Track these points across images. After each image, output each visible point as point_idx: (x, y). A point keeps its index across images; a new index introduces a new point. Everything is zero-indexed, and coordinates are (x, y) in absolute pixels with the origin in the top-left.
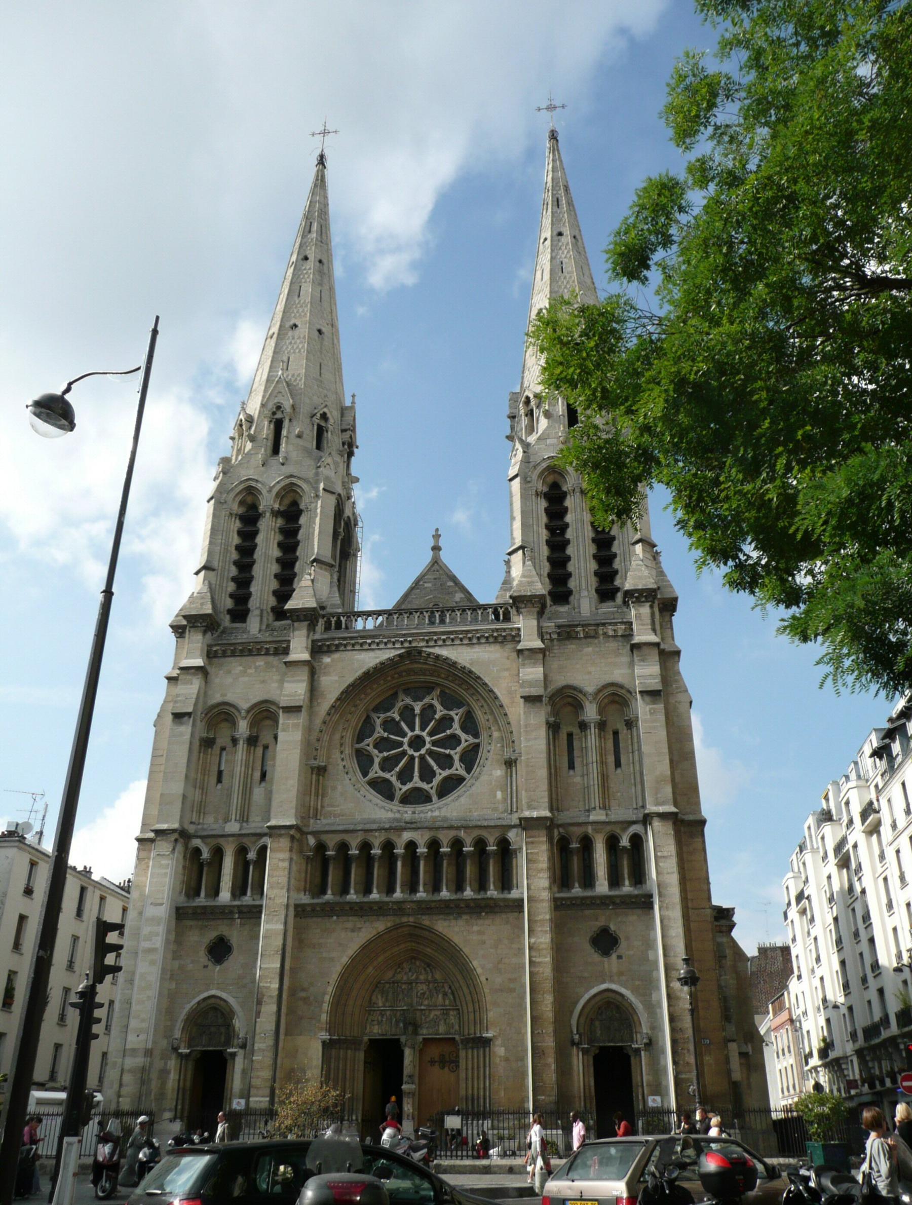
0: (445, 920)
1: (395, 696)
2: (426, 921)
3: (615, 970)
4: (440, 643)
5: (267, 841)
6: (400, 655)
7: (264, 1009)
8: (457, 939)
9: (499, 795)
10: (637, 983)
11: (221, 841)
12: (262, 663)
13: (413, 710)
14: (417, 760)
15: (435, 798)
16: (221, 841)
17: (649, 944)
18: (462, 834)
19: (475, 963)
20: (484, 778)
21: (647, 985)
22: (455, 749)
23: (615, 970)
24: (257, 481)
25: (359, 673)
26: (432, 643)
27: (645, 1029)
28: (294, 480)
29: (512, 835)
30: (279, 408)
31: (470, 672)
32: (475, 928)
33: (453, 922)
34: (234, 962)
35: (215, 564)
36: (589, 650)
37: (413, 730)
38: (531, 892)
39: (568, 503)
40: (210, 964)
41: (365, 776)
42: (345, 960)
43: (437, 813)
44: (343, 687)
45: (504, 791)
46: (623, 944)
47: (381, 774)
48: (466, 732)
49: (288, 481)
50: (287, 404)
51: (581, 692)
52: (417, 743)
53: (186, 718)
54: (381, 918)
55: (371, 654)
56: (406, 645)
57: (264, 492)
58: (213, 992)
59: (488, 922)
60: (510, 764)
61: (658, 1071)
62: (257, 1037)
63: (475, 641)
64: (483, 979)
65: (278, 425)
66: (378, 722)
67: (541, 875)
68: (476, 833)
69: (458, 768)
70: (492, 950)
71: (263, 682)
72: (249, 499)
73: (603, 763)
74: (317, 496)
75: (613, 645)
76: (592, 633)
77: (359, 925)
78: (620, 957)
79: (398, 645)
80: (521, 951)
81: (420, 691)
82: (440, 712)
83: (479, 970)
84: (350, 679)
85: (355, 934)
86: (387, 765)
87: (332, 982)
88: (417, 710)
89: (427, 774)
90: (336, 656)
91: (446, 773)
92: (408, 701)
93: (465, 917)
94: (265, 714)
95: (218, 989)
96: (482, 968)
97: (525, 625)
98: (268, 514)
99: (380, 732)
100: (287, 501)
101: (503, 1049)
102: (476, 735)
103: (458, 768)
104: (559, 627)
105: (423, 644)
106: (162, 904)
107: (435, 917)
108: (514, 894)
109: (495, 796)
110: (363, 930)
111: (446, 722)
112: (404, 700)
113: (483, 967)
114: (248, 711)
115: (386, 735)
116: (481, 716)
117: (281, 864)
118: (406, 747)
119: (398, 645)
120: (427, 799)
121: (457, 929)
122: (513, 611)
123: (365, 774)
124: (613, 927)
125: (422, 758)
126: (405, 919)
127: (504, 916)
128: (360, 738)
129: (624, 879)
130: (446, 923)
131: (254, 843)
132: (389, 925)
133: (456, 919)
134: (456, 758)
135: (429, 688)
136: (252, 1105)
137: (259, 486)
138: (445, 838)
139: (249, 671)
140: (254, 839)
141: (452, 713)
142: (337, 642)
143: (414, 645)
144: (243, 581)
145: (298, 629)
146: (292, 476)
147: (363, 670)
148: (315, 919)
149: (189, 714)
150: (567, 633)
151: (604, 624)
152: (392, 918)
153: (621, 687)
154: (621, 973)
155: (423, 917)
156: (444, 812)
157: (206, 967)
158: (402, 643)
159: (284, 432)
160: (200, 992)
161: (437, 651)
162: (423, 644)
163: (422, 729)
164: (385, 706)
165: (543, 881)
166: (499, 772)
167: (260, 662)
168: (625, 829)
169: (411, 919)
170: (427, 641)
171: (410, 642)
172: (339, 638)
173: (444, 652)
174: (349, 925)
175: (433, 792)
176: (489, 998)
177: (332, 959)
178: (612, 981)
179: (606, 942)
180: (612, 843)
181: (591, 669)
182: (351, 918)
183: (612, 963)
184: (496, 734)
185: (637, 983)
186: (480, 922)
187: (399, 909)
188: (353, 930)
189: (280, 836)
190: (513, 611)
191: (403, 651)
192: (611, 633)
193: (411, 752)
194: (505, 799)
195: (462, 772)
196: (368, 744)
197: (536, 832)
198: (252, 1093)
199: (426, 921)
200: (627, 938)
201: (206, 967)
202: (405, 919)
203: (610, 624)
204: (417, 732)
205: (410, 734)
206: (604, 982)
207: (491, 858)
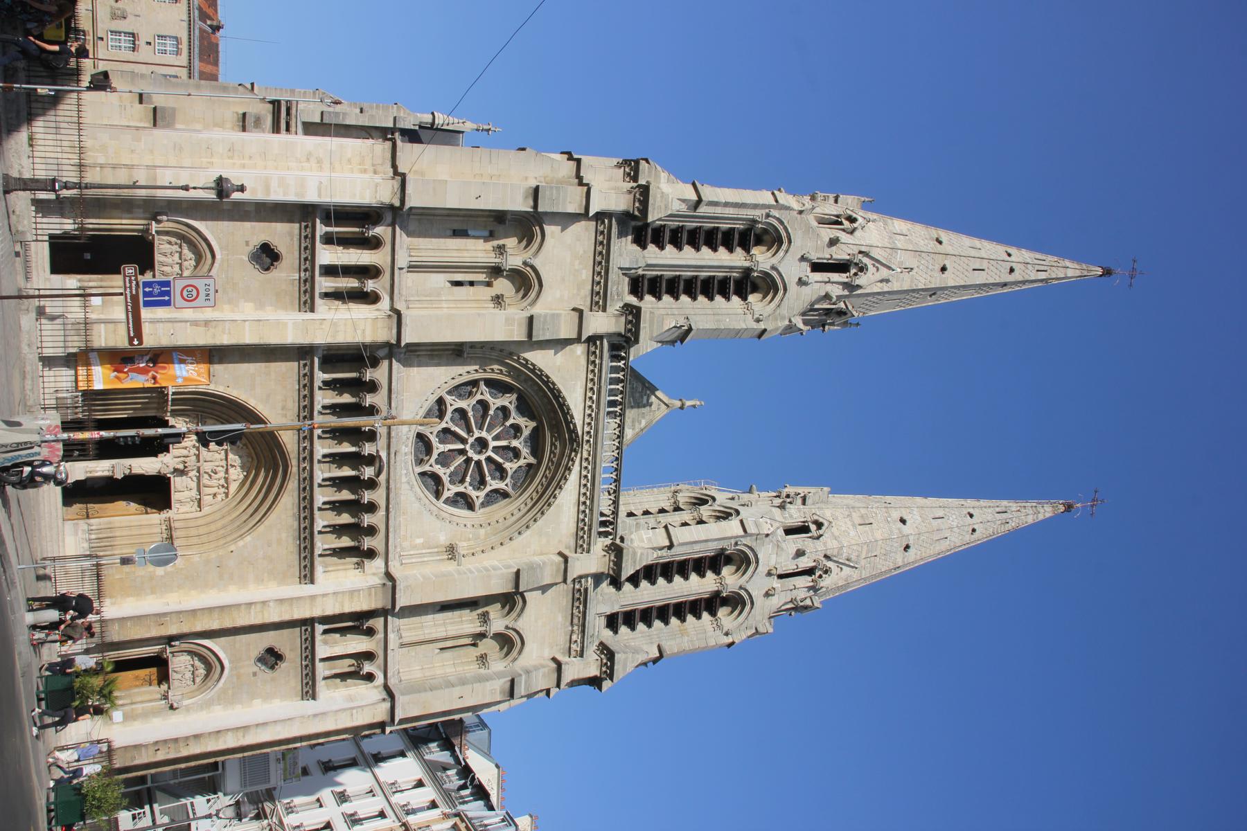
1: (532, 418)
2: (292, 485)
3: (242, 671)
4: (584, 473)
5: (385, 303)
6: (574, 431)
7: (202, 329)
9: (419, 541)
10: (230, 692)
11: (388, 247)
12: (584, 277)
13: (515, 437)
14: (461, 446)
15: (419, 469)
16: (387, 248)
17: (267, 698)
18: (381, 513)
19: (248, 539)
20: (438, 523)
21: (229, 699)
22: (471, 484)
23: (242, 671)
24: (787, 252)
25: (560, 386)
26: (585, 464)
27: (186, 702)
28: (781, 292)
29: (377, 565)
30: (861, 269)
31: (550, 505)
32: (284, 535)
33: (290, 513)
34: (253, 275)
35: (703, 210)
36: (560, 618)
37: (496, 438)
38: (319, 600)
39: (710, 575)
40: (250, 248)
41: (449, 393)
43: (404, 479)
44: (547, 371)
45: (424, 546)
46: (266, 674)
47: (450, 409)
48: (487, 495)
49: (781, 286)
50: (862, 280)
51: (519, 615)
52: (482, 444)
53: (531, 203)
55: (580, 398)
56: (586, 438)
57: (774, 261)
58: (218, 256)
60: (451, 551)
61: (146, 715)
62: (170, 325)
63: (582, 508)
64: (233, 548)
65: (841, 267)
66: (506, 404)
67: (337, 605)
68: (382, 527)
69: (451, 490)
71: (563, 279)
72: (766, 238)
73: (446, 639)
74: (758, 321)
75: (562, 640)
76: (576, 620)
78: (255, 674)
79: (587, 429)
80: (259, 580)
81: (536, 442)
82: (510, 466)
83: (241, 543)
84: (554, 378)
86: (462, 413)
88: (515, 443)
89: (444, 459)
90: (583, 362)
91: (446, 479)
92: (526, 432)
93: (296, 524)
94: (526, 282)
95: (222, 260)
97: (594, 560)
98: (747, 264)
99: (495, 402)
100: (758, 281)
102: (483, 505)
103: (451, 490)
104: (586, 590)
105: (585, 455)
106: (319, 195)
107: (296, 494)
108: (319, 570)
109: (418, 537)
111: (501, 472)
112: (527, 425)
114: (533, 267)
115: (491, 412)
116: (501, 509)
117: (359, 332)
118: (477, 434)
119: (587, 429)
120: (420, 462)
122: (608, 541)
123: (449, 393)
124: (283, 665)
125: (462, 452)
128: (490, 383)
129: (331, 669)
130: (290, 506)
131: (384, 288)
134: (461, 489)
135: (537, 451)
136: (95, 327)
137: (781, 253)
138: (377, 496)
139: (577, 262)
140: (388, 286)
141: (508, 480)
142: (597, 361)
143: (586, 447)
144: (678, 237)
145: (617, 322)
146: (785, 289)
147: (565, 393)
149: (536, 206)
150: (580, 599)
151: (583, 631)
153: (520, 652)
154: (239, 677)
155: (296, 482)
156: (405, 487)
157: (247, 243)
158: (589, 433)
159: (835, 277)
160: (218, 239)
161: (576, 469)
162: (585, 455)
163: (496, 449)
164: (524, 407)
165: (331, 609)
166: (443, 539)
167: (586, 274)
168: (379, 667)
170: (587, 459)
171: (588, 441)
172: (601, 364)
173: (573, 477)
175: (426, 468)
176: (213, 555)
178: (231, 669)
179: (272, 657)
180: (369, 656)
181: (543, 623)
183: (250, 667)
184: (482, 531)
185: (230, 692)
186: (291, 540)
187: (308, 456)
188: (283, 408)
189: (390, 329)
190: (608, 541)
191: (580, 433)
192: (574, 637)
193: (471, 440)
194: (415, 547)
195: (446, 494)
196: (484, 393)
197: (380, 595)
198: (111, 326)
199: (292, 485)
200: (273, 679)
201: (247, 243)
203: (583, 637)
204: (492, 444)
205: (490, 453)
206: (231, 662)
207: (358, 542)
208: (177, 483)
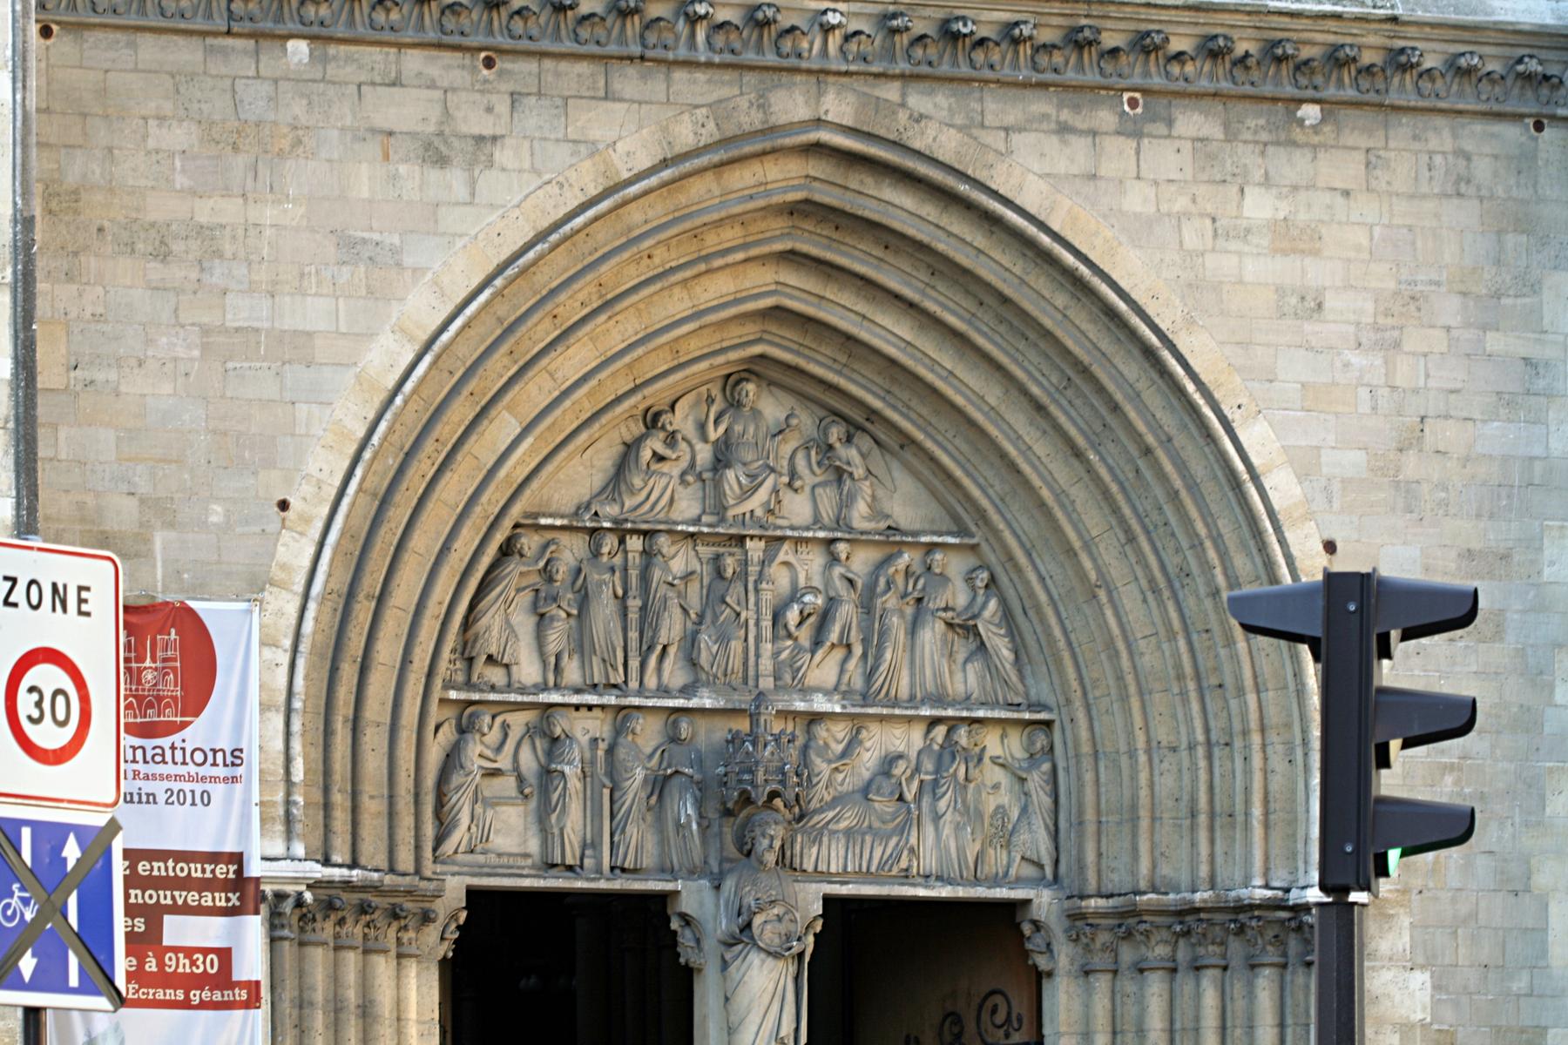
0: (1064, 129)
2: (935, 124)
8: (1137, 271)
19: (1259, 439)
32: (1259, 206)
33: (1118, 155)
42: (387, 356)
54: (628, 81)
59: (1342, 167)
70: (1356, 359)
77: (474, 122)
83: (1283, 487)
85: (455, 178)
87: (311, 505)
93: (1192, 122)
96: (1303, 476)
101: (1420, 980)
107: (997, 108)
110: (503, 155)
113: (1305, 466)
121: (1137, 200)
126: (791, 105)
127: (1441, 137)
132: (686, 135)
133: (1133, 130)
148: (150, 49)
152: (693, 87)
155: (918, 100)
169: (838, 106)
174: (408, 110)
177: (295, 347)
182: (414, 61)
186: (1292, 166)
188: (435, 154)
199: (935, 124)
202: (791, 105)
208: (844, 861)
